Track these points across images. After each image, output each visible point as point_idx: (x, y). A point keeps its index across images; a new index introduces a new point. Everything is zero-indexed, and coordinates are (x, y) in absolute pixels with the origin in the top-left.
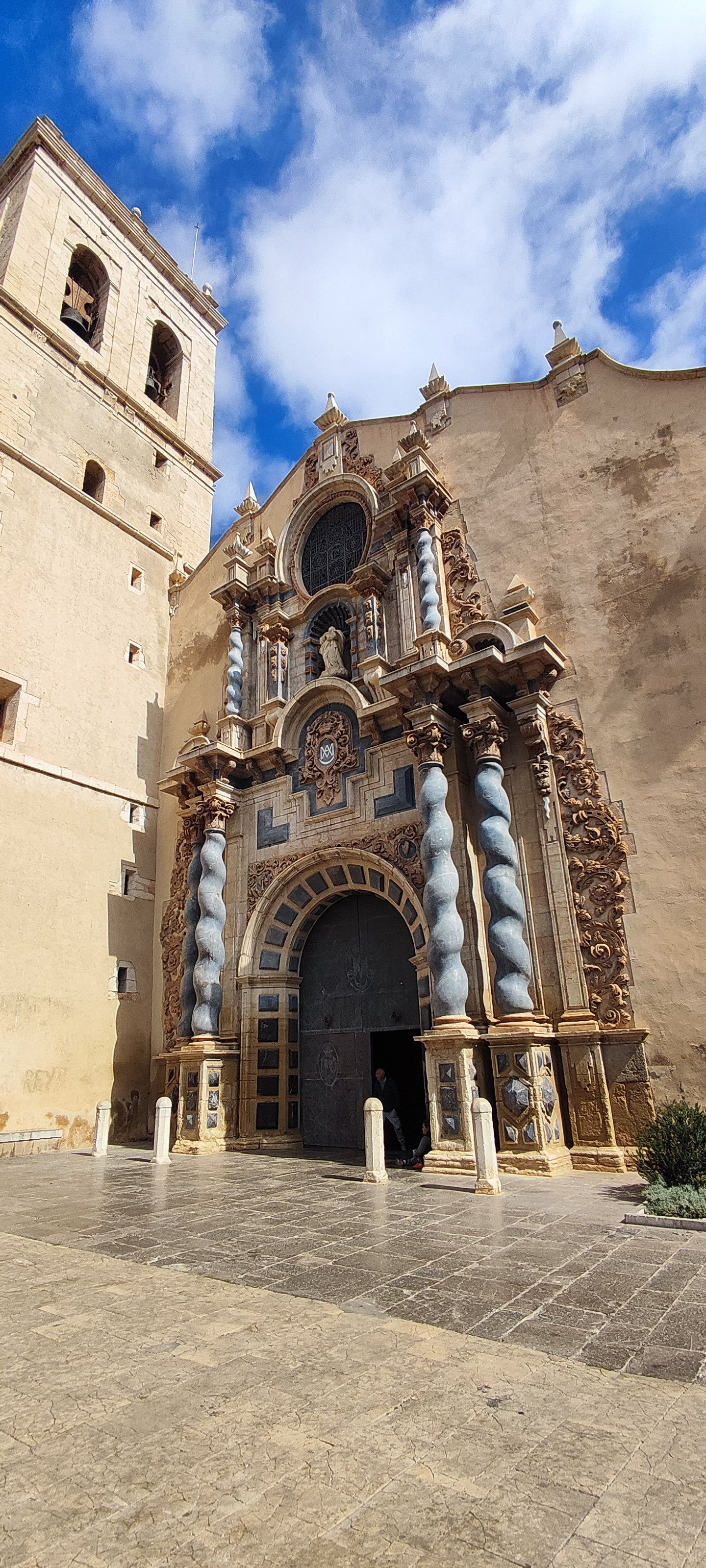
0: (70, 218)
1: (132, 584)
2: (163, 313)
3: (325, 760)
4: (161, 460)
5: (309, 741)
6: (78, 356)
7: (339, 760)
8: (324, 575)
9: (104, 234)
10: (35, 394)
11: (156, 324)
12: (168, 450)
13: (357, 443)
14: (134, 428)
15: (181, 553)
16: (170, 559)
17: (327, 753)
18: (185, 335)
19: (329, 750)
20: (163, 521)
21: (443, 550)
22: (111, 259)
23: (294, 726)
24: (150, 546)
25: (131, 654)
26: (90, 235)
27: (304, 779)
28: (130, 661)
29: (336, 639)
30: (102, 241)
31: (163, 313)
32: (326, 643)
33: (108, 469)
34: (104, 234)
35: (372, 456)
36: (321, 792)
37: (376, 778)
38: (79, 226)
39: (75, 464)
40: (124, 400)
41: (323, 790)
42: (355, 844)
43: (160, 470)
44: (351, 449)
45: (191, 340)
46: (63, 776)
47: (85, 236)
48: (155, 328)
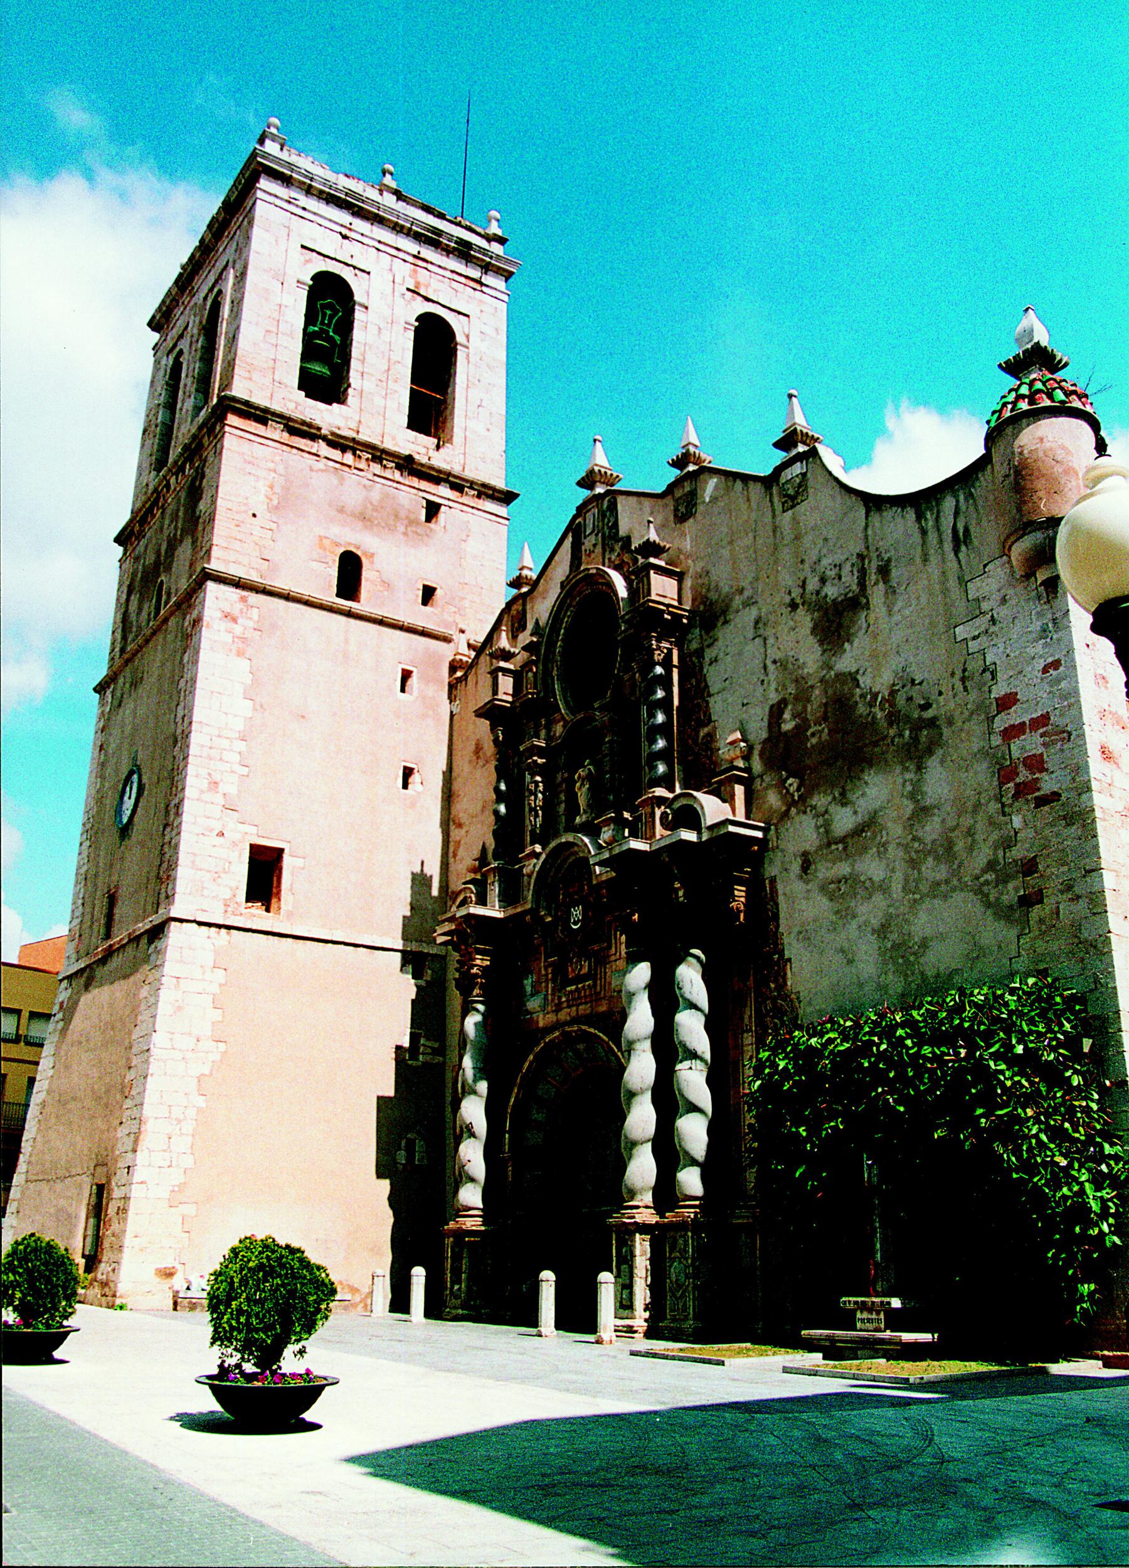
0: (303, 247)
2: (427, 299)
3: (575, 923)
4: (432, 510)
6: (319, 429)
9: (345, 237)
11: (417, 324)
15: (464, 627)
16: (447, 640)
18: (459, 313)
20: (438, 592)
24: (424, 633)
30: (346, 250)
31: (427, 299)
33: (365, 554)
34: (345, 237)
40: (379, 455)
43: (432, 525)
48: (417, 331)
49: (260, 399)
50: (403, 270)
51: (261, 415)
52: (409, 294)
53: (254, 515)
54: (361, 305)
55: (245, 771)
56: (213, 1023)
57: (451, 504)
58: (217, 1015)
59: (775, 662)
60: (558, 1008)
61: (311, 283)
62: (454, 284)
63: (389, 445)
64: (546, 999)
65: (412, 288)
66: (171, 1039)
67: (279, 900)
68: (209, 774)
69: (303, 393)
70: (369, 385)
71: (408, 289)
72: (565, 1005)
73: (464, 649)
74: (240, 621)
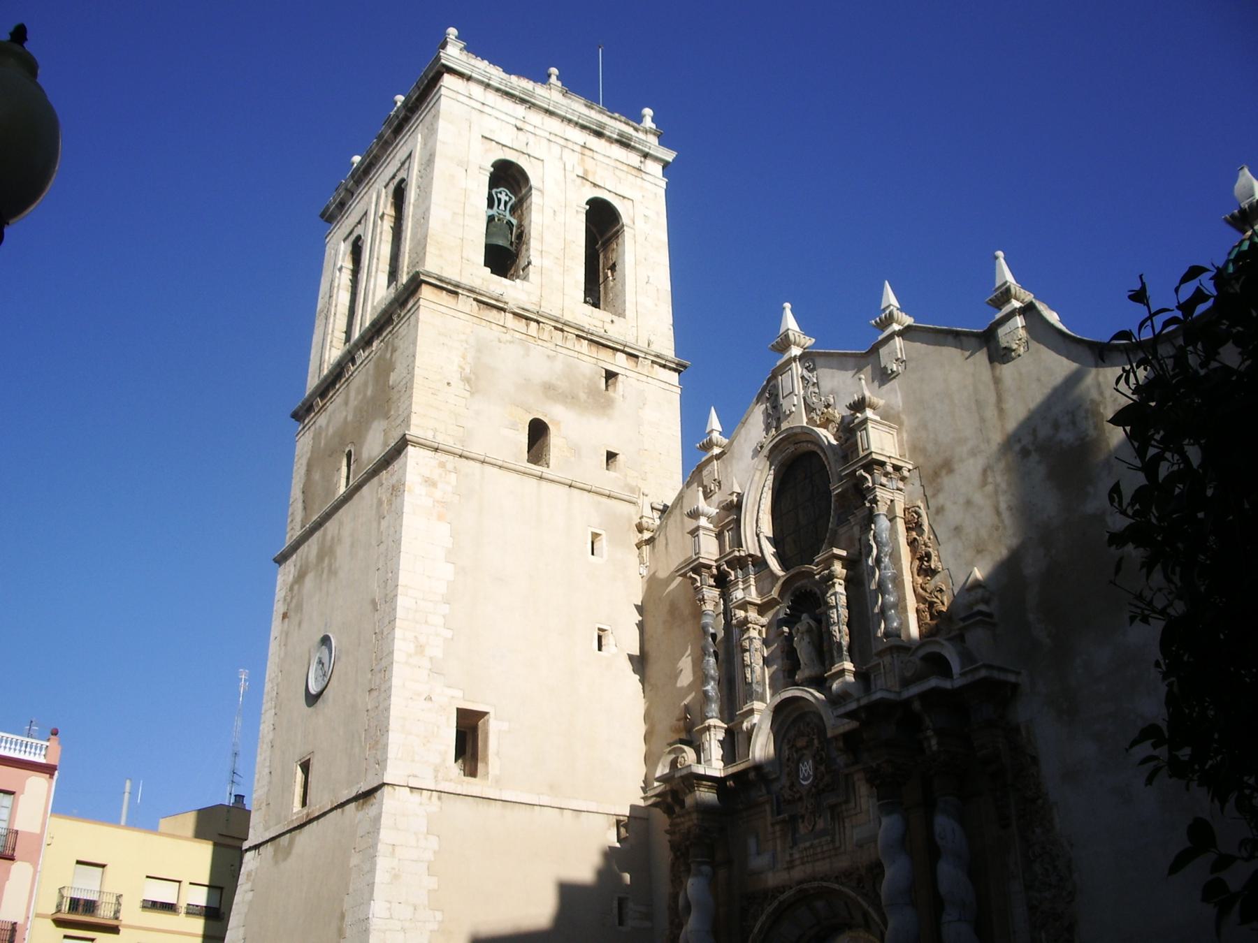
0: (483, 136)
1: (593, 554)
2: (595, 185)
6: (506, 303)
10: (468, 370)
12: (618, 363)
14: (576, 355)
15: (646, 492)
17: (806, 771)
18: (624, 197)
19: (808, 767)
21: (908, 529)
22: (529, 155)
25: (600, 638)
26: (504, 143)
28: (600, 649)
29: (809, 630)
31: (595, 185)
36: (803, 817)
37: (852, 805)
38: (492, 140)
39: (516, 432)
45: (633, 201)
46: (541, 804)
47: (500, 146)
48: (589, 215)
49: (451, 274)
50: (572, 159)
51: (451, 289)
52: (580, 180)
53: (448, 384)
54: (538, 190)
55: (449, 634)
56: (429, 891)
57: (628, 373)
58: (432, 883)
60: (791, 866)
61: (492, 169)
62: (618, 172)
63: (568, 317)
64: (774, 856)
65: (581, 175)
66: (389, 909)
67: (487, 764)
68: (416, 637)
69: (489, 270)
70: (547, 263)
71: (578, 176)
72: (798, 862)
73: (647, 511)
74: (440, 485)
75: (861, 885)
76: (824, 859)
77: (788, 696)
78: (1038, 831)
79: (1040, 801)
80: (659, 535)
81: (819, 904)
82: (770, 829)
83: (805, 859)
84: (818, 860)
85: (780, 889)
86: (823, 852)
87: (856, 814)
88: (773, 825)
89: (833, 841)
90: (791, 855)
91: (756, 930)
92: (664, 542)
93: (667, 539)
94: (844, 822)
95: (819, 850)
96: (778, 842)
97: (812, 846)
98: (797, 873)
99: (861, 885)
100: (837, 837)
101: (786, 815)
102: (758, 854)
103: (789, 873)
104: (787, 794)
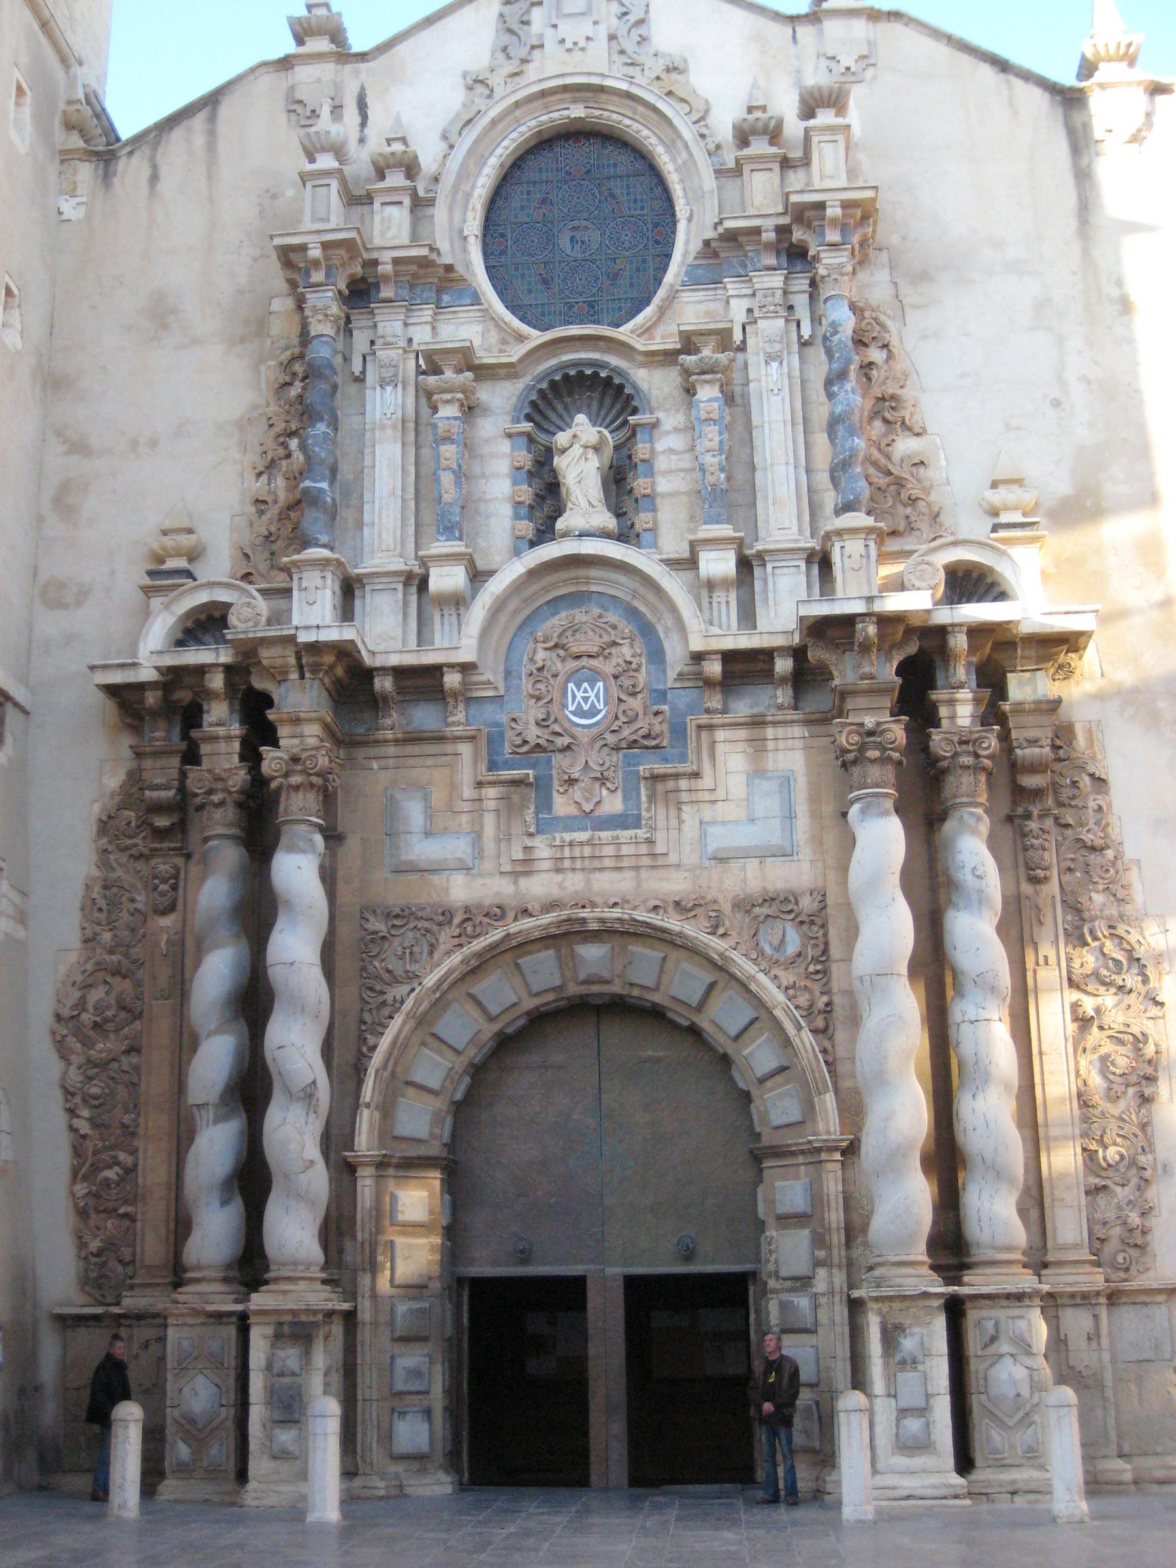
3: (580, 713)
5: (540, 664)
7: (618, 723)
8: (545, 282)
13: (647, 12)
17: (586, 699)
23: (503, 618)
27: (525, 742)
32: (577, 450)
35: (685, 61)
36: (572, 782)
37: (707, 781)
41: (576, 780)
42: (656, 908)
44: (632, 18)
59: (1086, 380)
60: (525, 867)
75: (721, 931)
76: (618, 869)
77: (584, 552)
78: (1098, 898)
79: (1110, 853)
80: (131, 153)
81: (592, 953)
82: (468, 792)
83: (567, 864)
84: (601, 869)
85: (498, 913)
86: (618, 857)
87: (713, 802)
88: (480, 785)
89: (650, 842)
90: (527, 849)
91: (430, 980)
92: (146, 172)
93: (155, 168)
94: (679, 809)
95: (608, 850)
96: (489, 821)
97: (589, 843)
98: (539, 886)
99: (721, 931)
100: (660, 837)
101: (530, 772)
102: (428, 834)
103: (516, 882)
104: (533, 734)
